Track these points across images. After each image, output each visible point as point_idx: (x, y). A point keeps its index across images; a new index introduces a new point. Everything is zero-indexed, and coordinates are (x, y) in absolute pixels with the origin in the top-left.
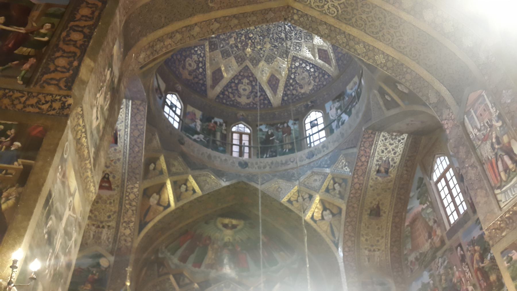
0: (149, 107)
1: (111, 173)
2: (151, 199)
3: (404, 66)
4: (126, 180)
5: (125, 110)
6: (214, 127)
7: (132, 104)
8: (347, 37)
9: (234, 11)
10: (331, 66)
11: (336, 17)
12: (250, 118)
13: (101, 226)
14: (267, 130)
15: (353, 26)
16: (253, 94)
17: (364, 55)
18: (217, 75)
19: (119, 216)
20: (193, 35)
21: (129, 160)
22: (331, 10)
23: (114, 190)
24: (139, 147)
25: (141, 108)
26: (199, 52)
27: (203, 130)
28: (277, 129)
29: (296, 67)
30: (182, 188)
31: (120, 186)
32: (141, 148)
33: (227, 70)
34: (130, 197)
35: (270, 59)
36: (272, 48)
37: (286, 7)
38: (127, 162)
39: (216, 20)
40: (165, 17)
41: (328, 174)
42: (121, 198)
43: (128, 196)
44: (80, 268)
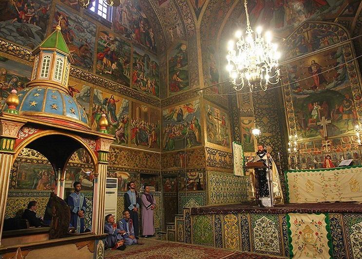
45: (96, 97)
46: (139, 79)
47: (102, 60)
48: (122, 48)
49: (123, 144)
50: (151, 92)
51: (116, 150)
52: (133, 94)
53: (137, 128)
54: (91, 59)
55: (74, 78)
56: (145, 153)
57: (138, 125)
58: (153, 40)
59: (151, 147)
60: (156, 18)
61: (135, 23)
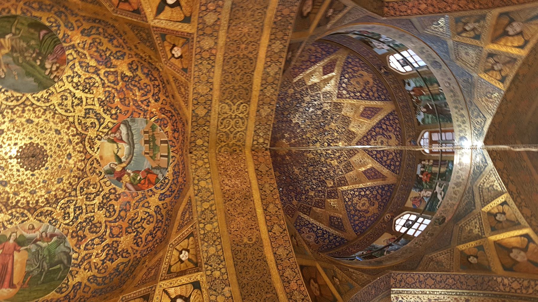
0: (397, 268)
3: (276, 20)
5: (404, 295)
6: (427, 175)
7: (396, 287)
8: (265, 86)
9: (259, 211)
10: (338, 58)
11: (248, 103)
12: (411, 134)
14: (422, 113)
15: (252, 85)
16: (385, 133)
17: (278, 64)
18: (372, 174)
20: (287, 255)
22: (243, 110)
25: (399, 278)
26: (350, 196)
27: (431, 187)
28: (418, 102)
29: (348, 93)
30: (501, 220)
33: (364, 165)
35: (346, 121)
36: (334, 121)
37: (253, 152)
39: (269, 231)
40: (267, 293)
41: (453, 41)
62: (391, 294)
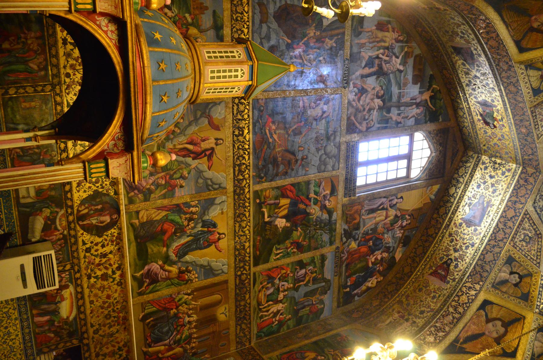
1: (456, 259)
2: (490, 325)
4: (468, 274)
7: (522, 173)
13: (406, 317)
19: (433, 317)
21: (485, 248)
23: (448, 282)
24: (505, 234)
25: (531, 180)
31: (457, 280)
32: (507, 236)
34: (460, 300)
38: (482, 249)
42: (449, 297)
43: (457, 295)
44: (346, 337)
45: (211, 202)
46: (277, 281)
47: (284, 196)
48: (321, 228)
49: (136, 284)
50: (262, 317)
51: (118, 273)
52: (243, 277)
53: (177, 308)
54: (277, 175)
55: (231, 154)
56: (128, 344)
57: (183, 308)
58: (364, 288)
59: (145, 353)
60: (406, 278)
61: (374, 240)
62: (517, 164)
